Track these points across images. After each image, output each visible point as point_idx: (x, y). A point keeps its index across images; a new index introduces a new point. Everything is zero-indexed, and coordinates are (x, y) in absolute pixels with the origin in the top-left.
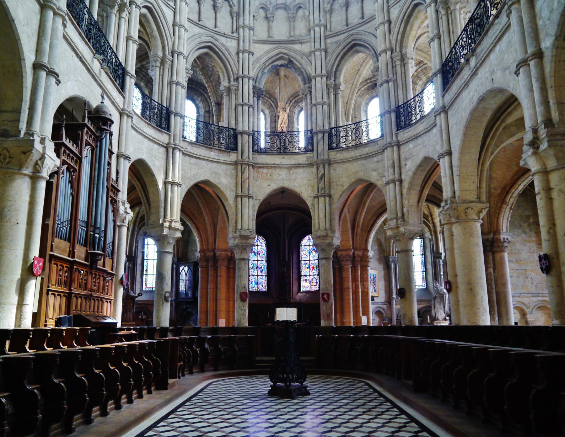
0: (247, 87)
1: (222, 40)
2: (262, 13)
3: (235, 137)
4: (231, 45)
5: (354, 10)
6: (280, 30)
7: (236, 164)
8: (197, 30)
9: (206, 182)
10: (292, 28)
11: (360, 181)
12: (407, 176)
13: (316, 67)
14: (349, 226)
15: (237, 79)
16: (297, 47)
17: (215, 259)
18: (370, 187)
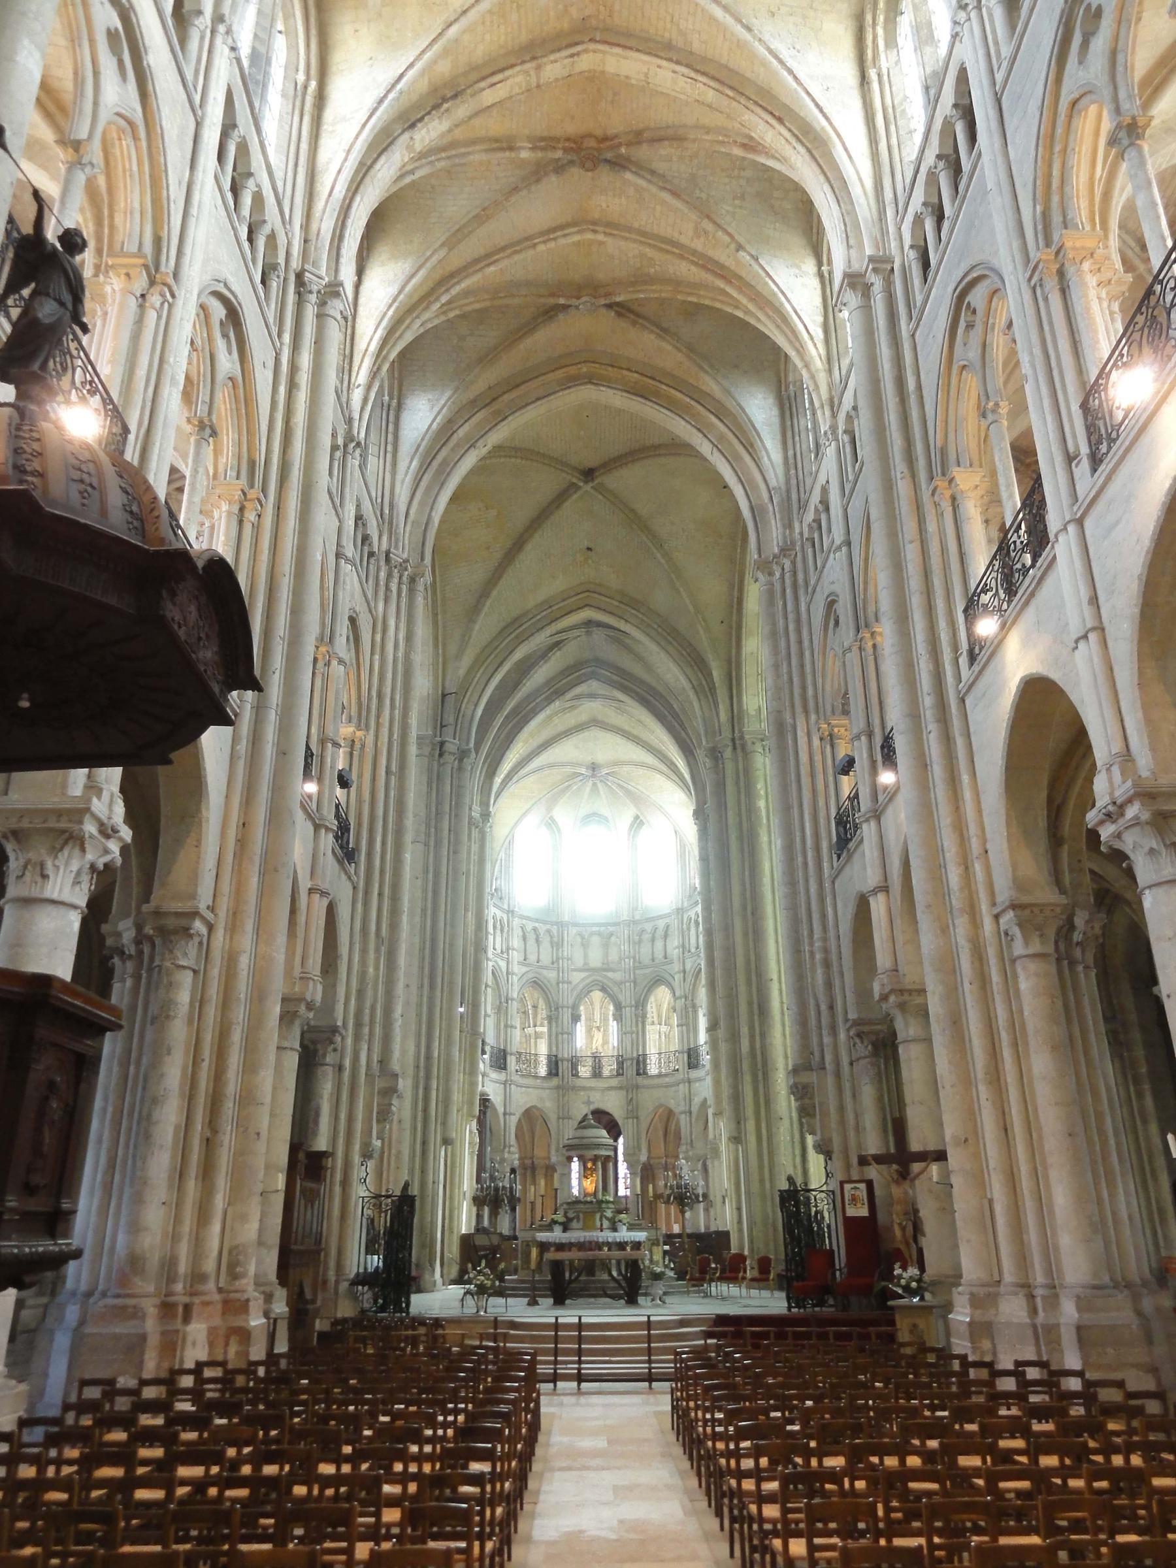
0: (566, 1015)
1: (545, 972)
2: (579, 939)
3: (557, 1063)
4: (552, 975)
5: (659, 944)
6: (595, 958)
7: (558, 1088)
8: (524, 969)
9: (534, 1107)
10: (606, 955)
11: (661, 1105)
12: (695, 1109)
13: (626, 997)
14: (661, 1133)
15: (557, 1009)
16: (610, 974)
17: (533, 1168)
18: (670, 1114)
